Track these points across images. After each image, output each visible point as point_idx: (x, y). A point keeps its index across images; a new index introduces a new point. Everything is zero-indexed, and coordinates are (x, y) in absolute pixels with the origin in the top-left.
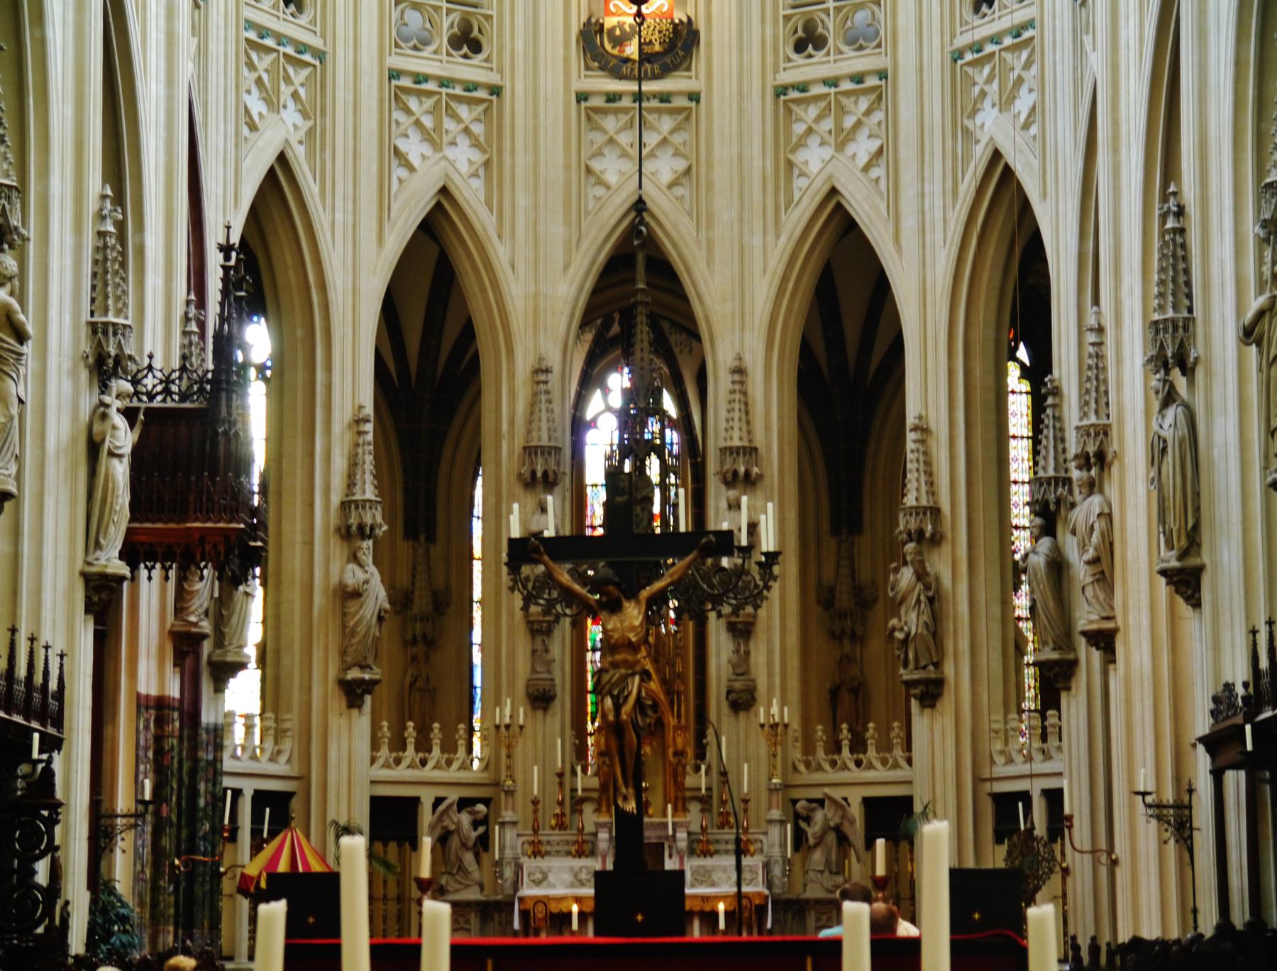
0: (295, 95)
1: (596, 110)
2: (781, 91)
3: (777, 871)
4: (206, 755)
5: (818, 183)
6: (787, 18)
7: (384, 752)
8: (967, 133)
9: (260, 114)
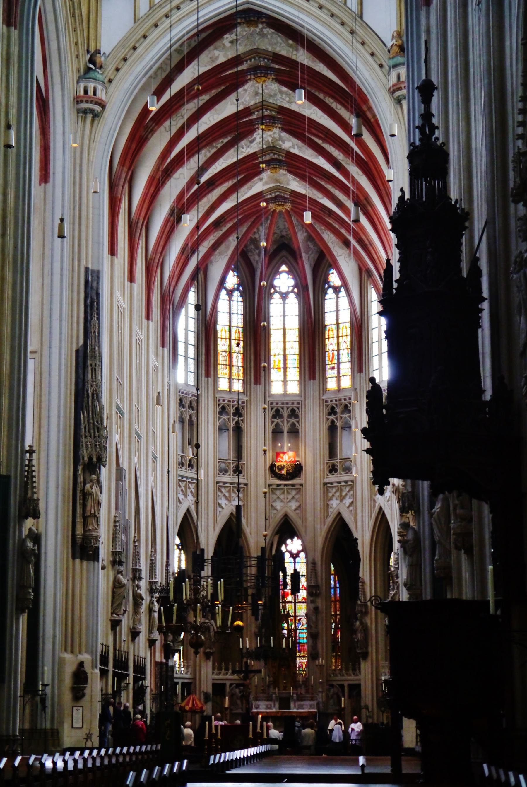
0: (191, 492)
1: (274, 489)
2: (325, 484)
3: (321, 705)
4: (170, 674)
5: (335, 511)
6: (327, 463)
7: (216, 671)
8: (374, 500)
9: (182, 499)
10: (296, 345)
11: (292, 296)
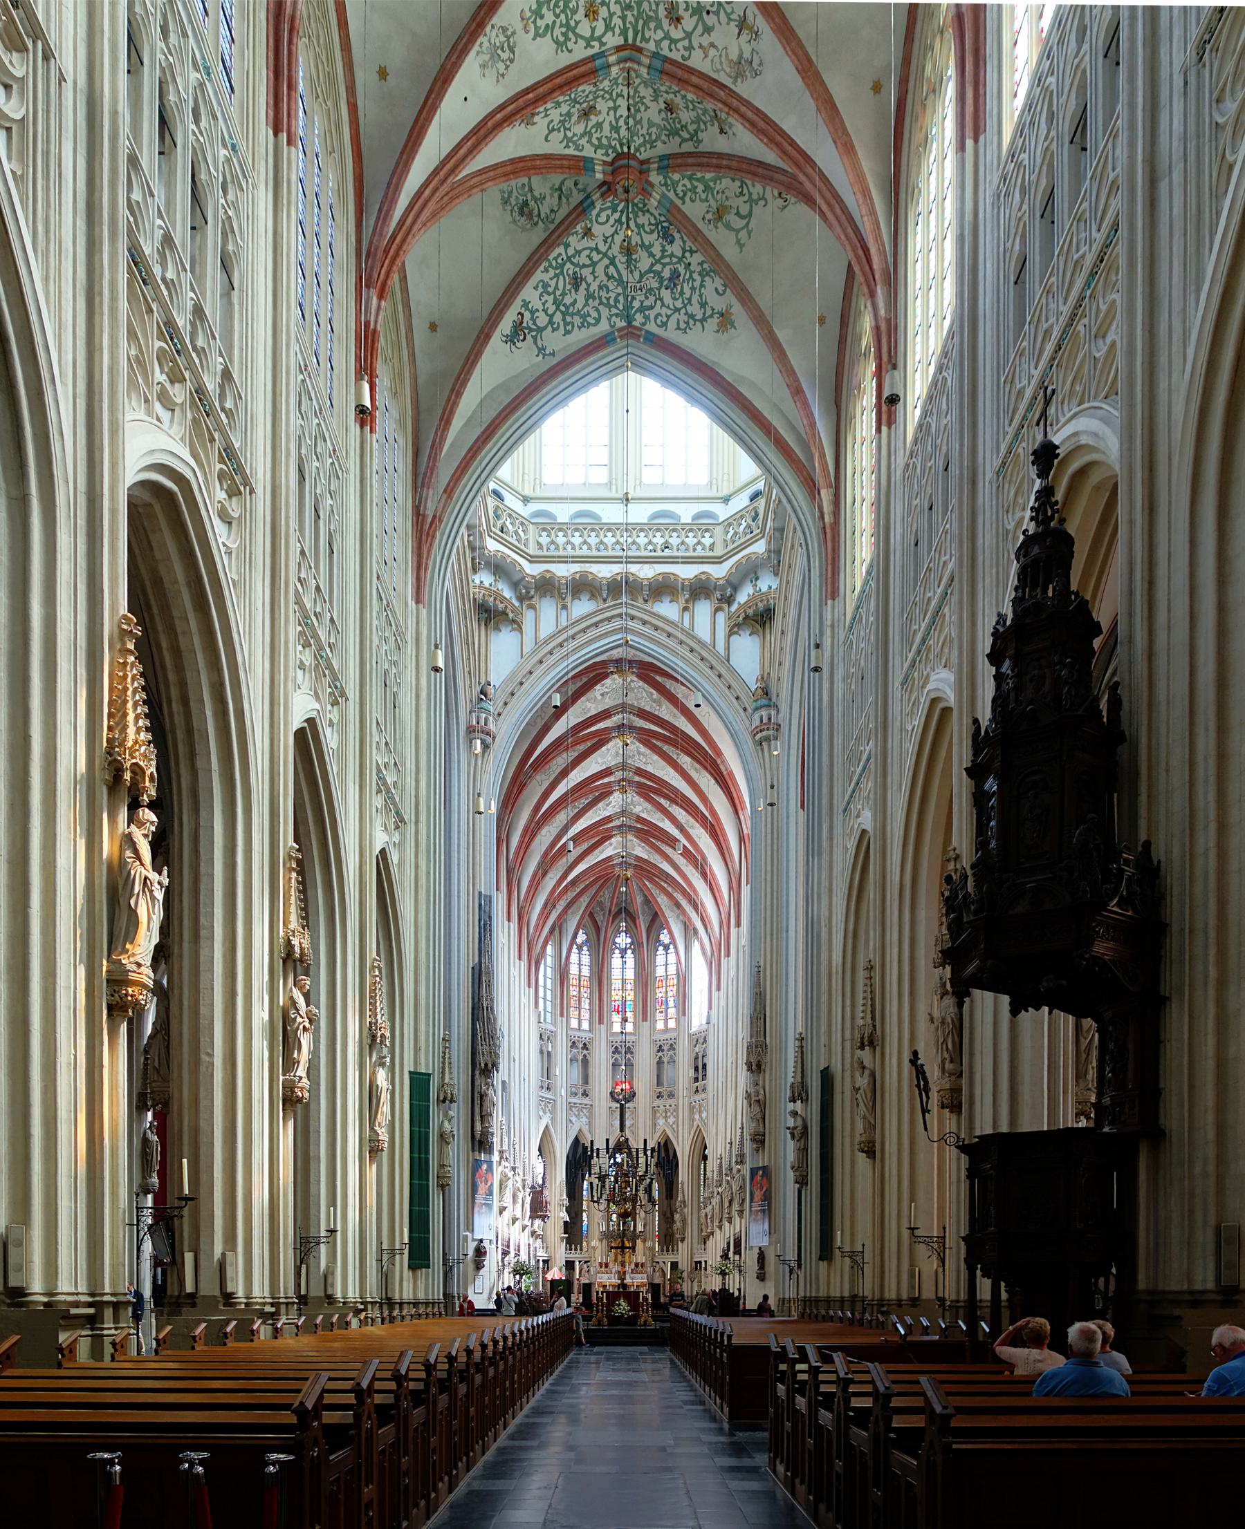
10: (632, 993)
11: (629, 952)
